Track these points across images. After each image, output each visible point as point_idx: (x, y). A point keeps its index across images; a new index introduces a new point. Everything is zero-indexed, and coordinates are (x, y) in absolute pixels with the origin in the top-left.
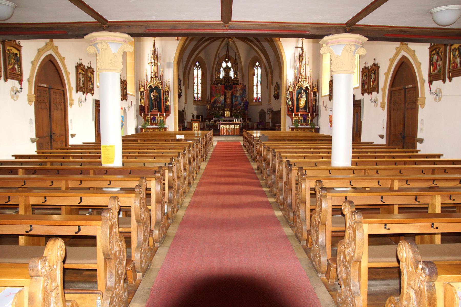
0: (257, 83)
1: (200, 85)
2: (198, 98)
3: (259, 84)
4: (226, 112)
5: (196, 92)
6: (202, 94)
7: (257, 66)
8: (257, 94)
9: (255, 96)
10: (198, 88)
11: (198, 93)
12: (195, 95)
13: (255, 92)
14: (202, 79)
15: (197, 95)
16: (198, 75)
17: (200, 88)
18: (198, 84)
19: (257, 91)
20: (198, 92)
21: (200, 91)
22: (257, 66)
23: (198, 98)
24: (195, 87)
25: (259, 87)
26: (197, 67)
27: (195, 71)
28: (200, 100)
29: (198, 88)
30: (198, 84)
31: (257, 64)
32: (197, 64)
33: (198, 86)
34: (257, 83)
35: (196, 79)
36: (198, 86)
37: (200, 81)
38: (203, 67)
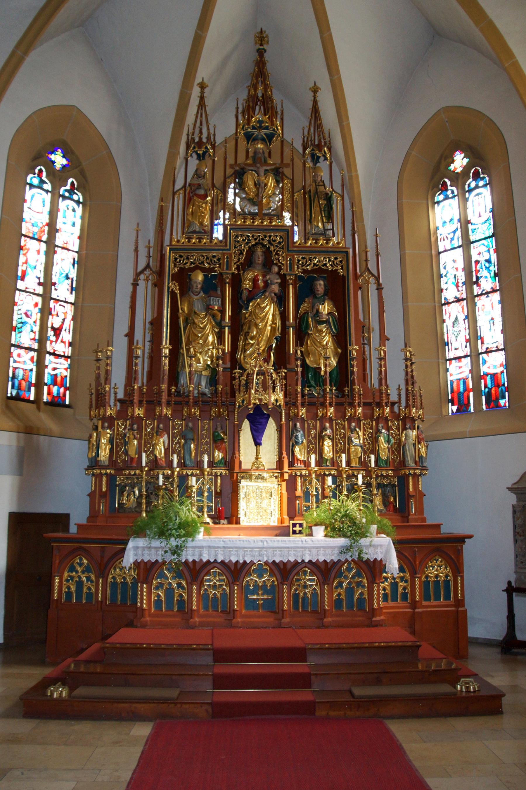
0: (472, 280)
1: (63, 291)
2: (39, 384)
3: (487, 283)
4: (245, 485)
5: (26, 337)
6: (75, 361)
7: (459, 179)
8: (475, 356)
9: (458, 372)
10: (46, 312)
12: (22, 362)
13: (457, 342)
14: (82, 262)
15: (41, 365)
16: (52, 228)
17: (63, 315)
18: (47, 283)
19: (474, 337)
20: (42, 340)
21: (67, 336)
22: (459, 179)
23: (39, 384)
24: (26, 305)
25: (490, 310)
26: (57, 177)
27: (36, 205)
28: (56, 403)
29: (46, 312)
30: (47, 283)
31: (459, 162)
32: (59, 160)
33: (46, 297)
34: (472, 280)
36: (46, 297)
37: (65, 264)
38: (89, 176)
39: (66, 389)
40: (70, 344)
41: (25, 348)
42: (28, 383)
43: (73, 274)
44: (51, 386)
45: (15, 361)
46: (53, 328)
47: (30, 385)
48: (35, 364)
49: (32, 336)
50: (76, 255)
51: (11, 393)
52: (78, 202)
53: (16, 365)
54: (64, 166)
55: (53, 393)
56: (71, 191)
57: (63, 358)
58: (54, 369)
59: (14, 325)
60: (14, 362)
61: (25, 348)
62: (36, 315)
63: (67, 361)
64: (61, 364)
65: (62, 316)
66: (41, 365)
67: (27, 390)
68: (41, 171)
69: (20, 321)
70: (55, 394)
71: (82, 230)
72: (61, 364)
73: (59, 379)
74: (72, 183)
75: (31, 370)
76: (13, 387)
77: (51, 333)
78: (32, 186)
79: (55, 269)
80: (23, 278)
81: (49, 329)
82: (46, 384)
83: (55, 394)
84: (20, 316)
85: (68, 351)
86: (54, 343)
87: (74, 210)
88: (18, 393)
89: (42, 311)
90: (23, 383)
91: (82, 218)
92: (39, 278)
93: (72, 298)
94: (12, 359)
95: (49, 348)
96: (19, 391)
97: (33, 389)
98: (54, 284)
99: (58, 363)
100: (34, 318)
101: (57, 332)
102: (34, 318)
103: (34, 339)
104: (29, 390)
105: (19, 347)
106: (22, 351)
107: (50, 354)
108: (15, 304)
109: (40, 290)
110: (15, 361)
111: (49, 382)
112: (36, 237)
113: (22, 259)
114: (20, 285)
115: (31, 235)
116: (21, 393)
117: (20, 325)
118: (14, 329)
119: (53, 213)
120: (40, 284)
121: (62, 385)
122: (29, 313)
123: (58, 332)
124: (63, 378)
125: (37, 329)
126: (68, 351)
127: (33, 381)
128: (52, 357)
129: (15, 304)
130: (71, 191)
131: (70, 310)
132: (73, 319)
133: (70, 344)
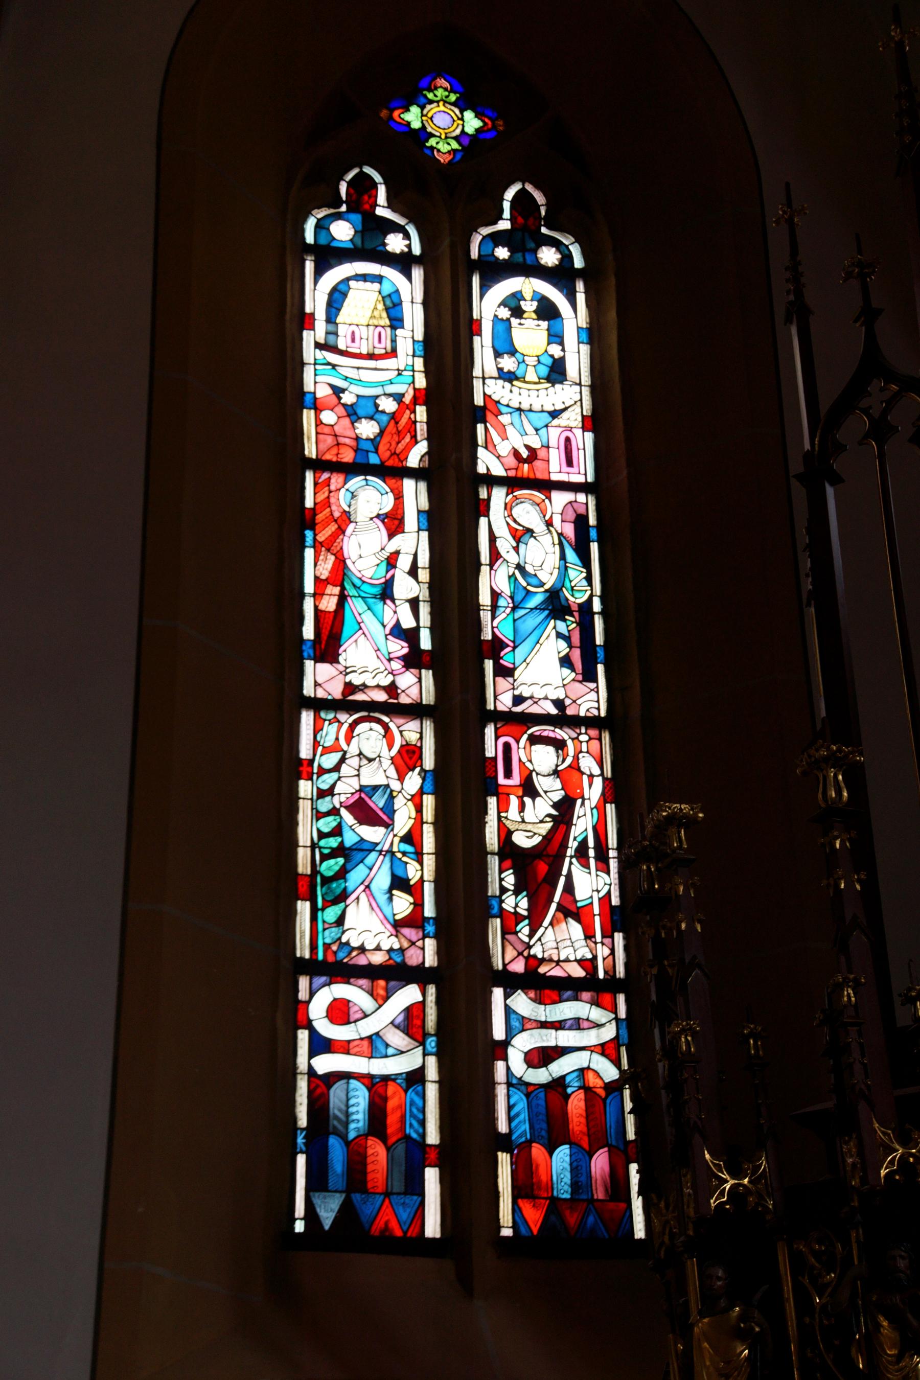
2: (468, 1144)
6: (648, 995)
10: (463, 783)
11: (459, 981)
12: (363, 1040)
15: (464, 1048)
16: (451, 403)
17: (555, 787)
18: (457, 648)
20: (460, 911)
23: (468, 1144)
24: (360, 766)
26: (445, 200)
27: (359, 333)
28: (575, 1235)
30: (457, 648)
32: (443, 121)
35: (373, 536)
39: (621, 1154)
40: (617, 919)
41: (371, 973)
42: (401, 1149)
43: (584, 587)
44: (537, 1151)
45: (320, 1045)
46: (509, 852)
47: (416, 1155)
48: (431, 1043)
49: (403, 904)
50: (587, 502)
51: (311, 1215)
52: (561, 276)
53: (325, 1064)
54: (470, 144)
55: (550, 1185)
56: (524, 239)
57: (586, 995)
58: (542, 1057)
59: (303, 864)
60: (312, 1054)
61: (371, 973)
62: (410, 803)
63: (614, 1010)
64: (577, 1024)
65: (551, 789)
66: (464, 1048)
67: (398, 1185)
68: (363, 186)
69: (333, 842)
70: (563, 1188)
71: (598, 388)
72: (577, 1024)
73: (576, 1104)
74: (522, 202)
75: (416, 1078)
76: (317, 1182)
77: (501, 878)
78: (329, 255)
79: (493, 581)
80: (328, 648)
81: (494, 863)
82: (505, 1143)
83: (563, 1188)
84: (327, 824)
85: (611, 955)
86: (524, 929)
87: (547, 311)
88: (347, 1212)
89: (441, 781)
90: (377, 1151)
91: (593, 335)
92: (411, 636)
93: (592, 700)
94: (303, 1036)
95: (502, 955)
96: (357, 1197)
97: (432, 1176)
98: (497, 645)
99: (558, 1026)
100: (403, 819)
101: (538, 870)
102: (403, 819)
103: (415, 920)
104: (417, 1188)
105: (339, 969)
106: (355, 994)
107: (511, 983)
108: (302, 769)
109: (417, 686)
110: (320, 1045)
111: (523, 1128)
112: (374, 459)
113: (314, 566)
114: (319, 678)
115: (348, 456)
116: (368, 1207)
117: (330, 867)
118: (308, 887)
119: (448, 344)
120: (414, 660)
121: (600, 1133)
122: (378, 801)
123: (542, 868)
124: (600, 1098)
125: (422, 871)
126: (611, 955)
127: (433, 1137)
128: (522, 1003)
129: (302, 769)
130: (524, 239)
131: (593, 761)
132: (615, 791)
133: (617, 919)
